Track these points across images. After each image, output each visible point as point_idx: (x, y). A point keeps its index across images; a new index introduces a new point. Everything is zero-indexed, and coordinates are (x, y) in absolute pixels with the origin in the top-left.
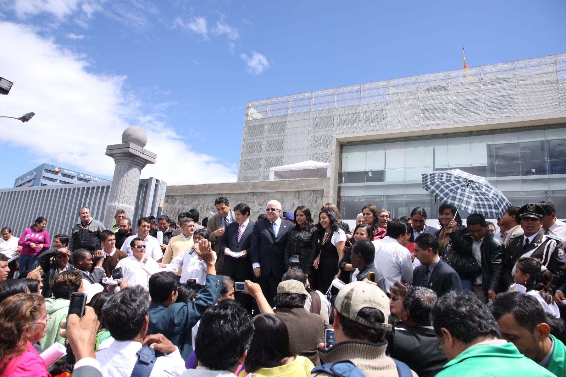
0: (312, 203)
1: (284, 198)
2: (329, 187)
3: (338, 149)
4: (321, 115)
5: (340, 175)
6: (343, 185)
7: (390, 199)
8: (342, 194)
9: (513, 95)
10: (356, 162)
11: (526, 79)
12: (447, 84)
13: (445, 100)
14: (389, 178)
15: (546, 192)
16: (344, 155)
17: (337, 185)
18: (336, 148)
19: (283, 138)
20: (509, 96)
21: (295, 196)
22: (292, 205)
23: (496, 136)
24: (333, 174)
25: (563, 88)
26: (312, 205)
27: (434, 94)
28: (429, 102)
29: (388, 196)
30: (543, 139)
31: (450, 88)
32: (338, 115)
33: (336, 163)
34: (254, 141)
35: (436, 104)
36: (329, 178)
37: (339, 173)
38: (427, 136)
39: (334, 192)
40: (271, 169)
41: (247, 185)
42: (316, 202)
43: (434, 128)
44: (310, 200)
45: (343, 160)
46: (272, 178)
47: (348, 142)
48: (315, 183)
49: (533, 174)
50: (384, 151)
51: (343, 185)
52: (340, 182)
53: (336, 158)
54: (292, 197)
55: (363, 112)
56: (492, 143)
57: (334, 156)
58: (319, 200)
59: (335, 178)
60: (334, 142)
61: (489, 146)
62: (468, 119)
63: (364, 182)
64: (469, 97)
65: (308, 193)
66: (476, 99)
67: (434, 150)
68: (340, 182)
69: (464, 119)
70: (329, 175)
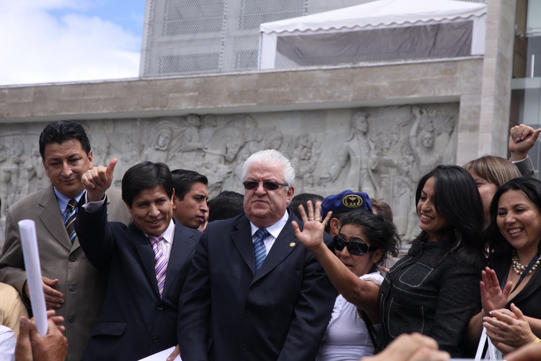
0: (418, 150)
1: (312, 136)
2: (477, 90)
5: (522, 46)
6: (532, 83)
17: (509, 84)
21: (352, 125)
22: (342, 159)
26: (417, 160)
36: (480, 59)
40: (265, 27)
41: (178, 88)
42: (430, 149)
44: (407, 143)
46: (268, 59)
48: (424, 78)
51: (532, 83)
52: (520, 70)
54: (343, 130)
58: (441, 140)
59: (501, 58)
65: (402, 116)
68: (520, 70)
70: (479, 44)
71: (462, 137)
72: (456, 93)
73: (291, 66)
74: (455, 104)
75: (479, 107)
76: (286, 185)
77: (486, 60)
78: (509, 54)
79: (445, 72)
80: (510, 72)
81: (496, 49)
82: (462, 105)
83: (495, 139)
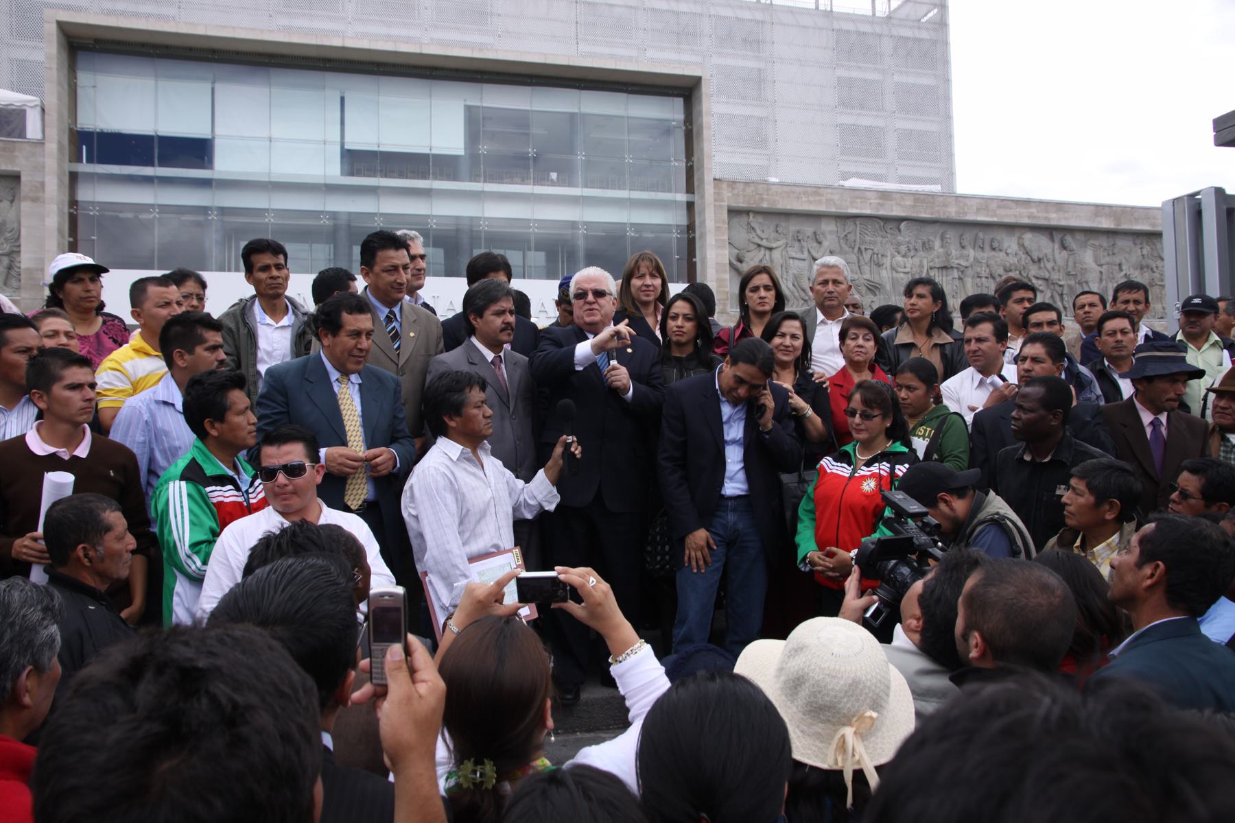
2: (41, 168)
3: (65, 56)
7: (227, 219)
8: (85, 194)
10: (131, 104)
14: (225, 164)
15: (573, 225)
16: (83, 78)
18: (59, 52)
24: (53, 133)
29: (223, 211)
33: (59, 99)
36: (41, 143)
37: (71, 130)
39: (59, 186)
45: (79, 91)
47: (97, 41)
49: (553, 184)
50: (208, 86)
53: (60, 84)
56: (478, 104)
57: (55, 73)
59: (60, 143)
61: (468, 109)
62: (395, 31)
63: (152, 165)
67: (342, 99)
69: (383, 30)
70: (33, 129)
71: (25, 206)
72: (16, 169)
74: (15, 178)
75: (43, 184)
77: (47, 145)
78: (66, 142)
79: (4, 149)
80: (67, 157)
81: (56, 137)
82: (23, 178)
83: (60, 211)
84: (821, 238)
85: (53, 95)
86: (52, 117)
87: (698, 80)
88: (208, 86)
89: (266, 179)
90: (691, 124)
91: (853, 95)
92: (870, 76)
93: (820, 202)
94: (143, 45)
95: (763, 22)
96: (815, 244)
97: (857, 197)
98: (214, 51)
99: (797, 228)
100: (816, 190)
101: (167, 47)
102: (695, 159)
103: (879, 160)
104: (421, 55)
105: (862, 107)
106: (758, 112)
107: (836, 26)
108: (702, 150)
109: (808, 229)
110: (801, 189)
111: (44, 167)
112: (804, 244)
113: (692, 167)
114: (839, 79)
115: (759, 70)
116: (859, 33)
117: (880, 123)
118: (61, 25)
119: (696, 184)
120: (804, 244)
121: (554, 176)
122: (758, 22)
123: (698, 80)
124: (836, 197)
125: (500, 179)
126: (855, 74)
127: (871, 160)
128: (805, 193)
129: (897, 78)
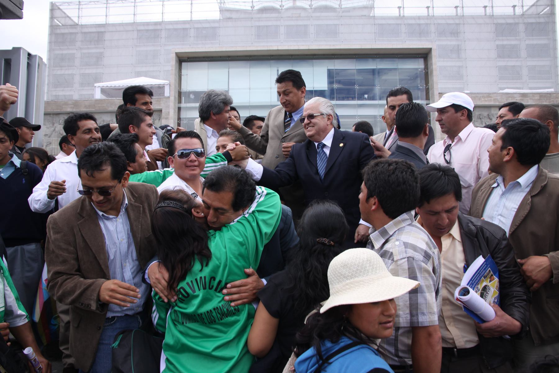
2: (168, 107)
3: (178, 65)
4: (146, 28)
5: (180, 94)
6: (183, 105)
8: (183, 115)
9: (339, 25)
11: (349, 11)
12: (280, 6)
13: (278, 23)
16: (184, 72)
17: (177, 105)
19: (102, 50)
20: (336, 25)
23: (337, 61)
24: (173, 93)
25: (378, 24)
27: (268, 15)
28: (262, 24)
30: (374, 67)
31: (283, 11)
32: (166, 29)
33: (175, 80)
34: (65, 52)
35: (269, 26)
36: (169, 97)
38: (272, 56)
39: (174, 113)
41: (66, 104)
43: (280, 48)
45: (182, 77)
46: (98, 95)
47: (188, 58)
49: (366, 99)
51: (183, 105)
52: (180, 102)
53: (175, 75)
55: (194, 28)
56: (333, 68)
57: (174, 71)
60: (174, 55)
64: (300, 23)
66: (307, 25)
70: (167, 94)
73: (104, 97)
74: (161, 111)
75: (169, 112)
76: (322, 114)
78: (177, 96)
82: (163, 111)
83: (174, 122)
84: (491, 117)
85: (173, 79)
86: (173, 87)
87: (430, 50)
88: (227, 70)
89: (248, 105)
90: (428, 69)
91: (504, 52)
92: (513, 43)
93: (491, 101)
94: (204, 57)
95: (459, 24)
96: (489, 120)
97: (509, 97)
98: (229, 57)
99: (480, 113)
100: (489, 95)
101: (212, 57)
102: (430, 84)
103: (518, 81)
104: (309, 50)
105: (509, 57)
106: (458, 64)
107: (495, 22)
108: (433, 80)
109: (485, 113)
110: (481, 95)
111: (169, 106)
112: (483, 120)
113: (428, 88)
114: (497, 46)
115: (458, 45)
116: (507, 24)
117: (518, 64)
118: (177, 54)
119: (430, 96)
120: (483, 120)
121: (366, 96)
122: (457, 24)
123: (430, 50)
124: (499, 98)
125: (343, 99)
126: (505, 43)
127: (515, 81)
128: (483, 97)
129: (527, 42)
